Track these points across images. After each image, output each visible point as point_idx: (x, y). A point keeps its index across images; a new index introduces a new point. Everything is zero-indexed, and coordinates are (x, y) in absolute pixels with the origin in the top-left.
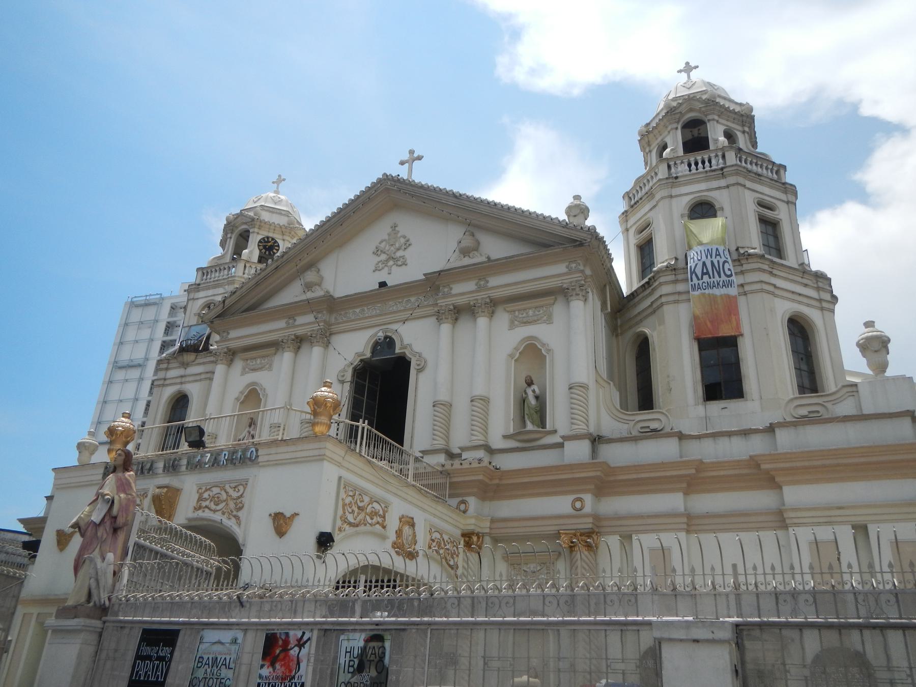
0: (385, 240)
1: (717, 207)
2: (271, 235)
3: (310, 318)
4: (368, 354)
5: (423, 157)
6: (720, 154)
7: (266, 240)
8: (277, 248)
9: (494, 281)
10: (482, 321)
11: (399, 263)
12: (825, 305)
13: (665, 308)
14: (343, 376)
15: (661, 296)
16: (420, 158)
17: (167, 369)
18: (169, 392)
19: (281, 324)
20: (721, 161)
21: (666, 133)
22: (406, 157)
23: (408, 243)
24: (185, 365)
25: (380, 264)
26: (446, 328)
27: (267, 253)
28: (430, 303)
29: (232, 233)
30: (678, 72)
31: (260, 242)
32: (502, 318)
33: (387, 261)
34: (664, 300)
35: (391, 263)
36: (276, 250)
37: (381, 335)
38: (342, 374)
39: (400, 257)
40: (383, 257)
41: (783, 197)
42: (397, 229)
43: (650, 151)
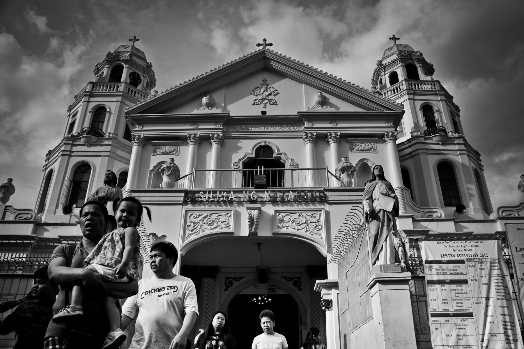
0: (258, 88)
2: (137, 71)
4: (254, 156)
5: (273, 45)
6: (433, 83)
7: (134, 74)
8: (140, 81)
11: (272, 103)
12: (481, 167)
13: (421, 156)
14: (237, 166)
15: (418, 149)
17: (73, 145)
18: (74, 161)
20: (433, 87)
21: (397, 66)
22: (262, 42)
23: (276, 92)
25: (257, 101)
27: (134, 82)
28: (297, 130)
29: (110, 65)
30: (389, 39)
31: (130, 74)
33: (263, 100)
34: (420, 151)
35: (265, 102)
36: (140, 82)
37: (263, 144)
38: (236, 164)
39: (271, 99)
42: (267, 82)
43: (385, 75)
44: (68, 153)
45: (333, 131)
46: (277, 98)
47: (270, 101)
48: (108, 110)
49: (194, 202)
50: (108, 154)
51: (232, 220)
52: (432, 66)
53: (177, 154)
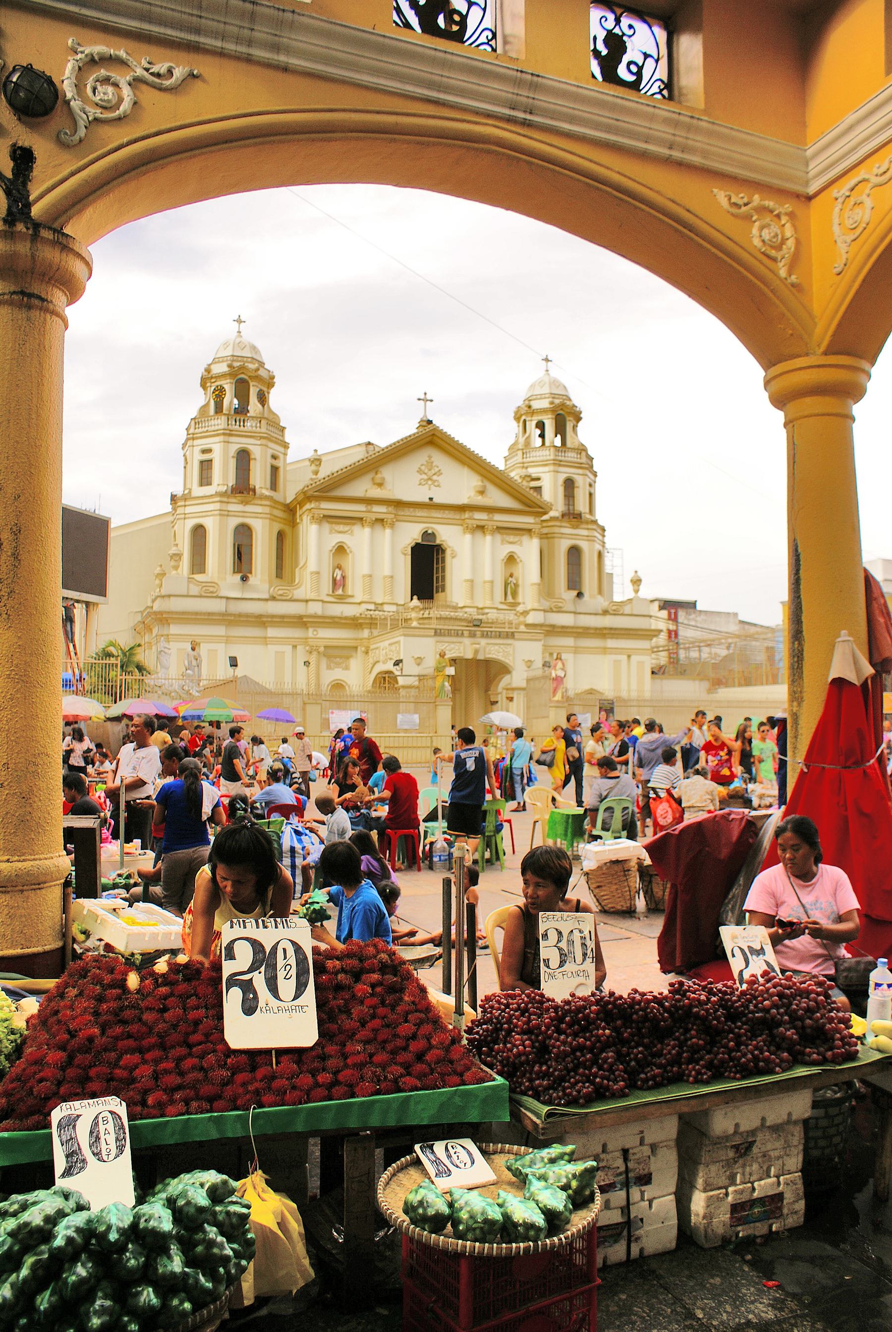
1: (576, 485)
3: (382, 509)
4: (420, 541)
9: (498, 517)
10: (488, 538)
13: (556, 540)
16: (431, 401)
18: (234, 522)
19: (362, 507)
22: (422, 397)
24: (245, 503)
26: (468, 537)
32: (498, 537)
35: (430, 482)
37: (430, 532)
40: (425, 477)
41: (592, 477)
44: (226, 513)
45: (490, 523)
46: (440, 479)
47: (435, 481)
48: (252, 456)
49: (441, 635)
50: (268, 516)
51: (462, 648)
52: (581, 413)
53: (352, 534)
